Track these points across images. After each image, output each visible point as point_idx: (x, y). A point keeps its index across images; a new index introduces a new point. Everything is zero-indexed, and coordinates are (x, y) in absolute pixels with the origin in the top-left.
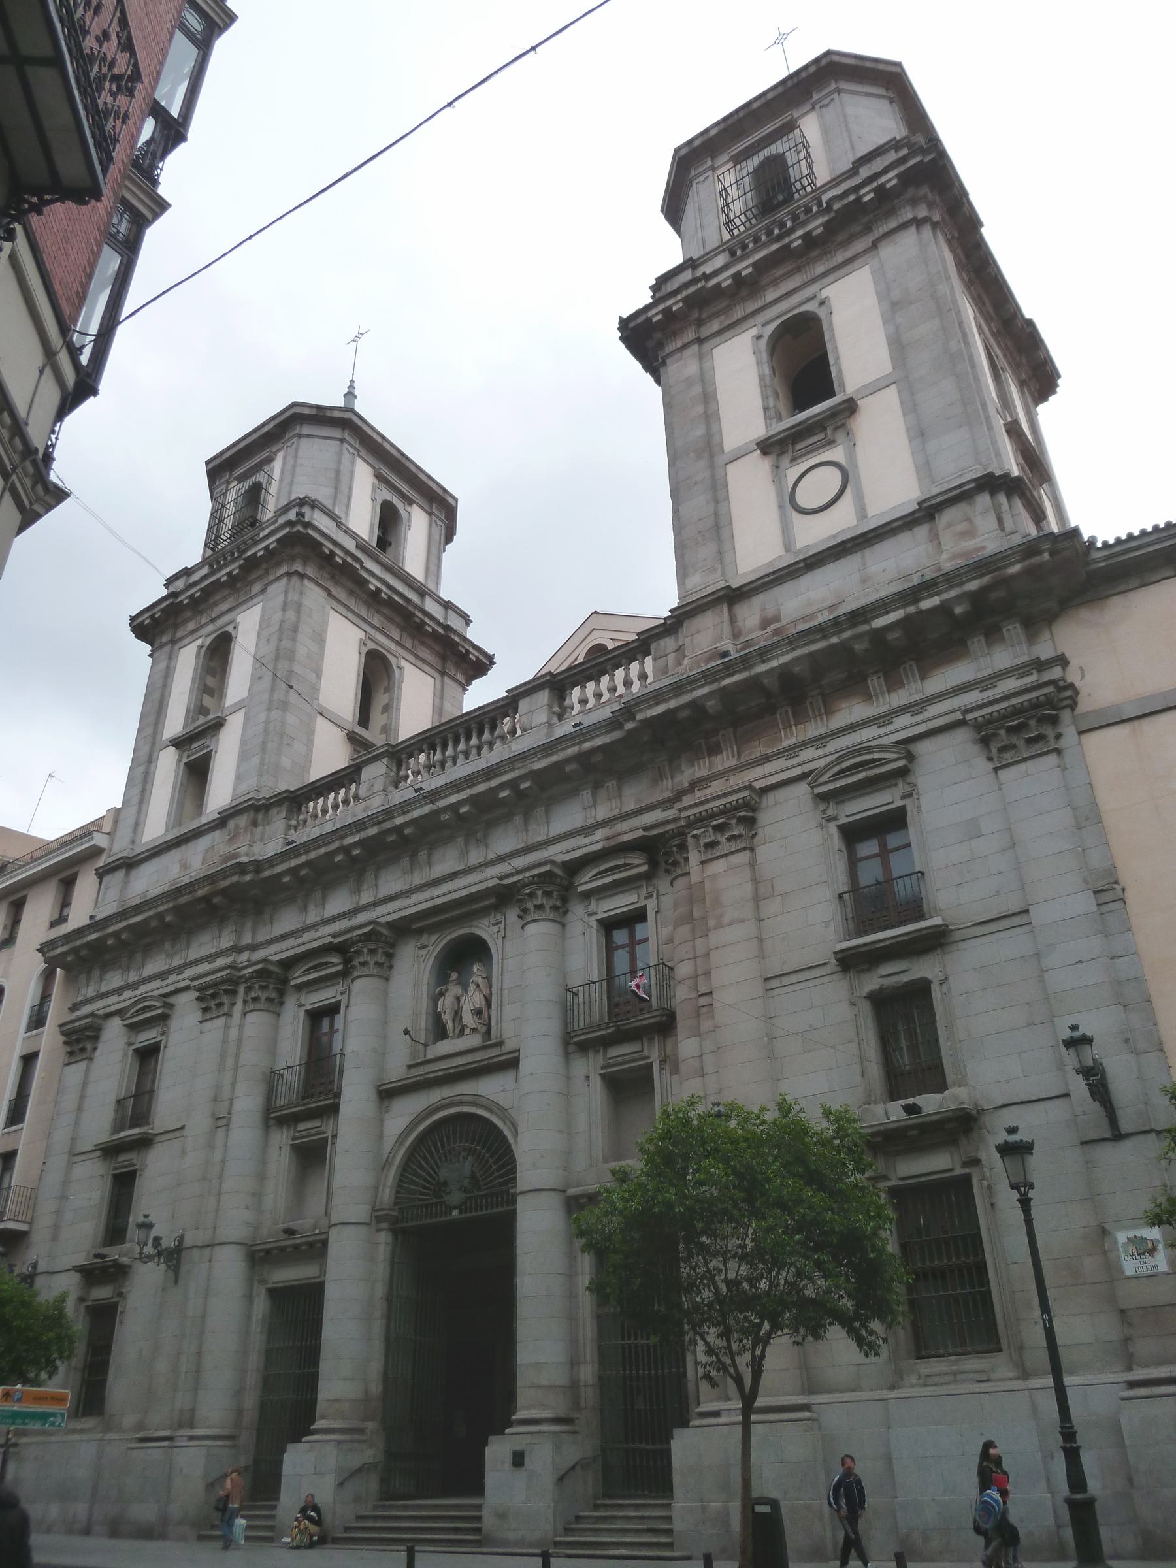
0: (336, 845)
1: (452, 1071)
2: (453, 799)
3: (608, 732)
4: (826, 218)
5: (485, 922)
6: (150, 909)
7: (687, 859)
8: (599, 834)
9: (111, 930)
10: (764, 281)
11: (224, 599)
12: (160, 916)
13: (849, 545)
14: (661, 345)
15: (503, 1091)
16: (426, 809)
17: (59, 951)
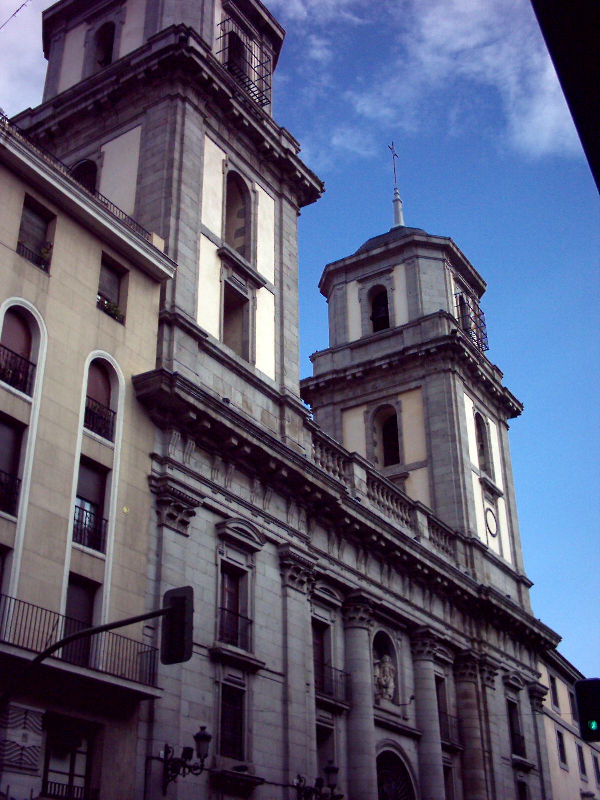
0: (379, 530)
1: (392, 723)
2: (428, 563)
3: (474, 590)
4: (502, 393)
5: (395, 634)
6: (279, 453)
7: (476, 676)
8: (450, 633)
9: (245, 435)
10: (480, 385)
11: (247, 147)
12: (281, 465)
13: (506, 569)
14: (453, 360)
15: (410, 750)
16: (418, 556)
17: (191, 400)
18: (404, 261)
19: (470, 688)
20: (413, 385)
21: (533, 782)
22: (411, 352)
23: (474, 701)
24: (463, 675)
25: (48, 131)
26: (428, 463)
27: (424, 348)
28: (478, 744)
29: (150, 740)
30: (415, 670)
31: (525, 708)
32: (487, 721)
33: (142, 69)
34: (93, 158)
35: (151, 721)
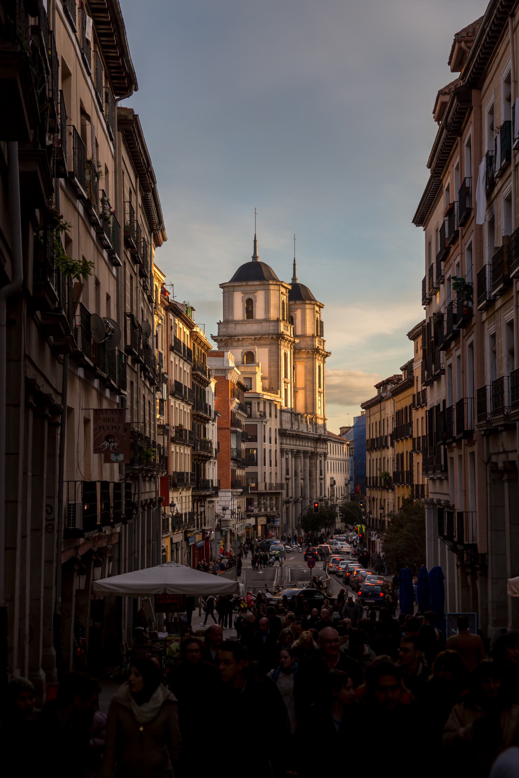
18: (301, 309)
19: (313, 461)
20: (302, 360)
21: (323, 481)
22: (303, 351)
23: (314, 465)
24: (312, 458)
25: (239, 339)
26: (305, 388)
27: (307, 351)
28: (314, 476)
29: (282, 498)
30: (304, 461)
31: (323, 461)
32: (316, 470)
33: (270, 336)
34: (252, 351)
35: (282, 494)
